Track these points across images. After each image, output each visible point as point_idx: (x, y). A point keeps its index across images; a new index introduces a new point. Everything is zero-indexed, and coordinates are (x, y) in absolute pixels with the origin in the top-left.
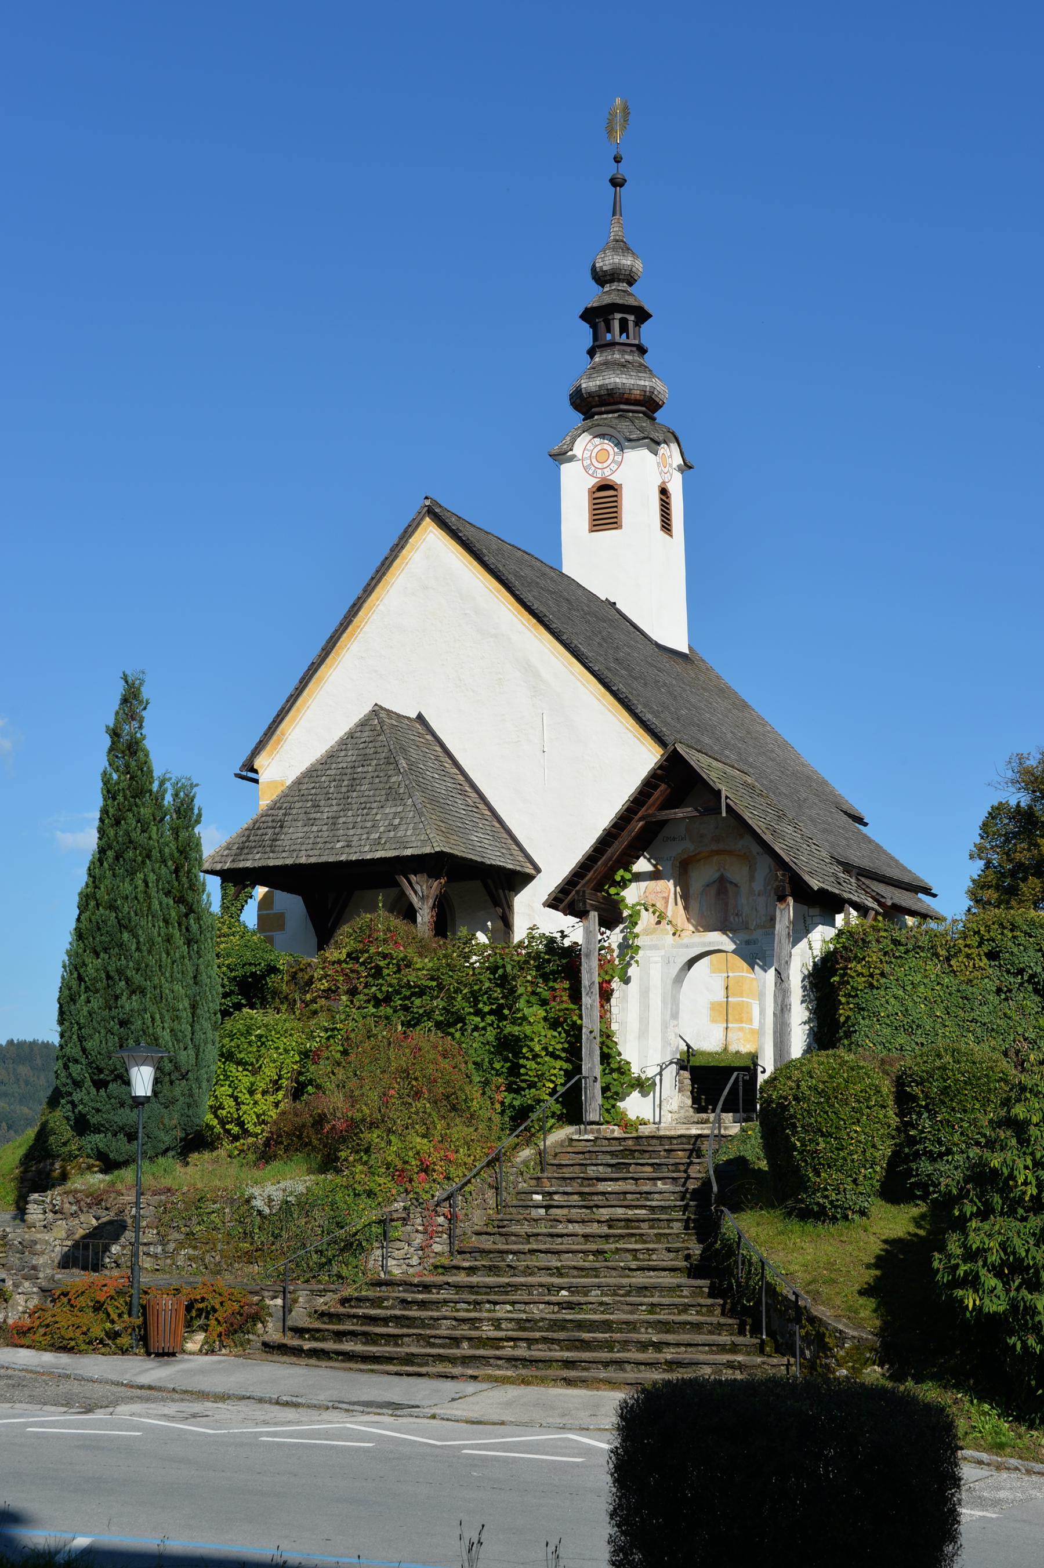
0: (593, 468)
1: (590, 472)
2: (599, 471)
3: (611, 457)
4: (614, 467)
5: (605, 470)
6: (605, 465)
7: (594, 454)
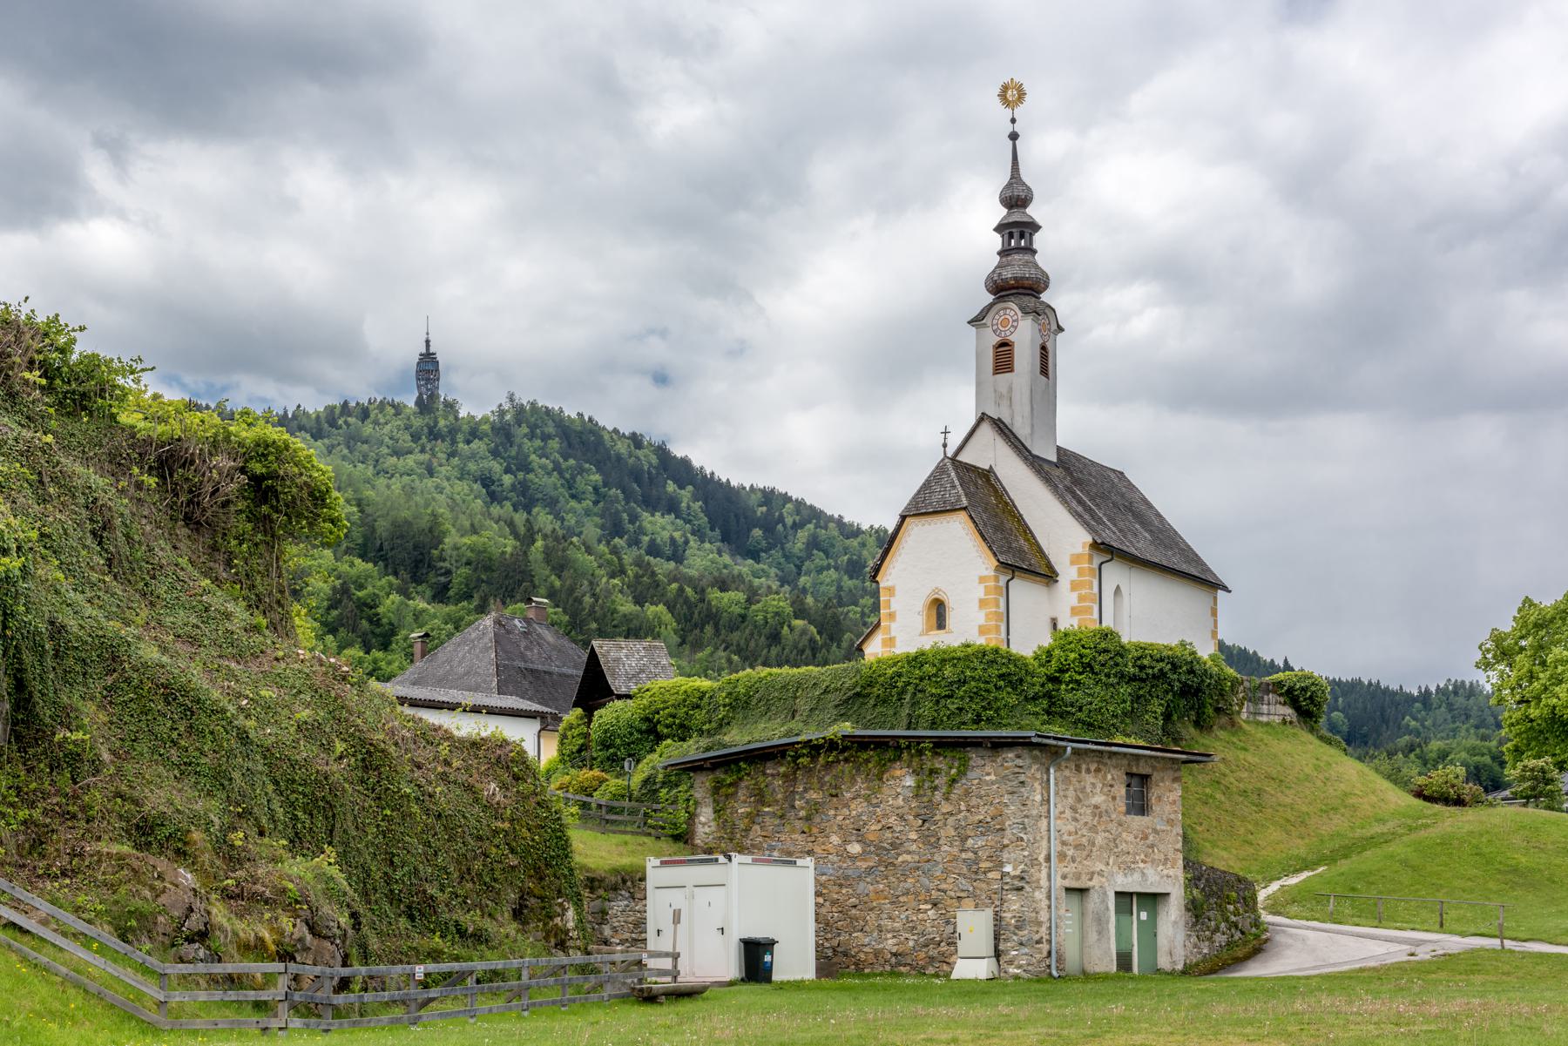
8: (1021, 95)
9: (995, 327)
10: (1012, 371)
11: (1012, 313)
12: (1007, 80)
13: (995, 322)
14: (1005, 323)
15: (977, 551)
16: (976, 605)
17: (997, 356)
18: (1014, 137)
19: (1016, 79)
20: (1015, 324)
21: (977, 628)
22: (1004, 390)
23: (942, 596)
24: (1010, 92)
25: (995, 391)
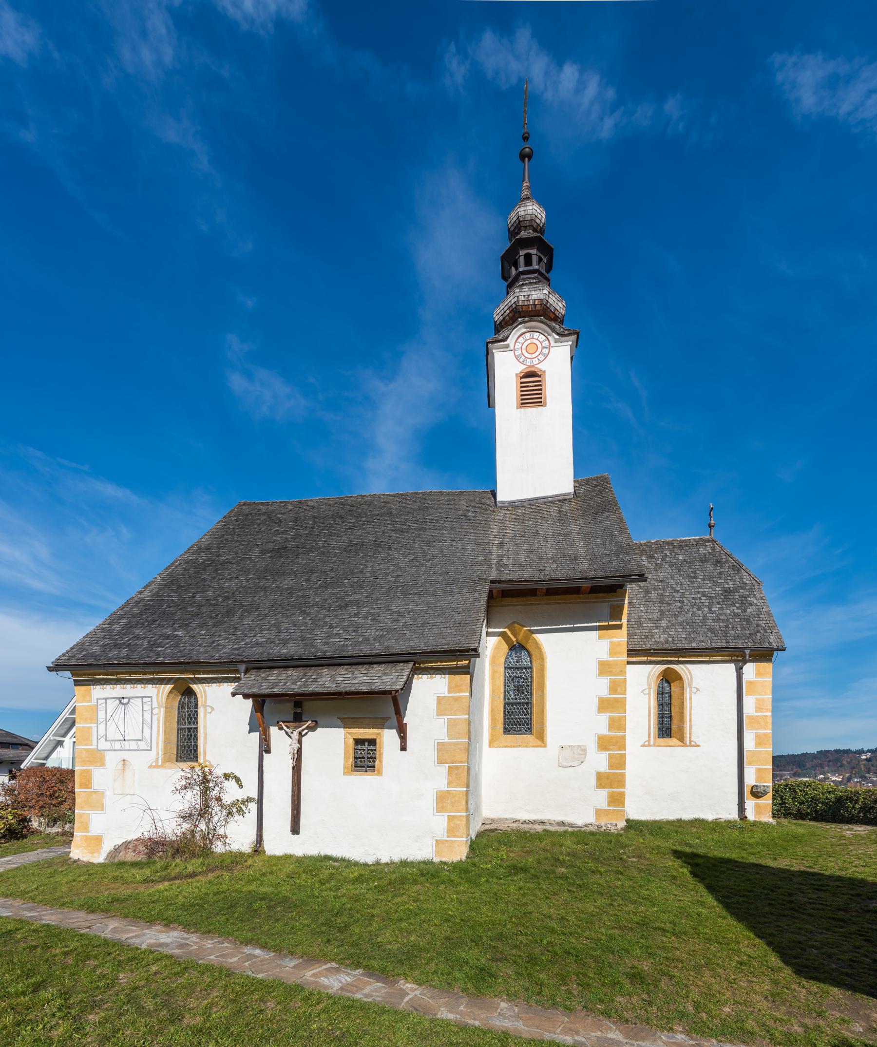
0: (523, 358)
2: (528, 360)
3: (539, 350)
4: (541, 357)
5: (534, 360)
6: (534, 356)
7: (524, 347)
9: (518, 353)
13: (518, 346)
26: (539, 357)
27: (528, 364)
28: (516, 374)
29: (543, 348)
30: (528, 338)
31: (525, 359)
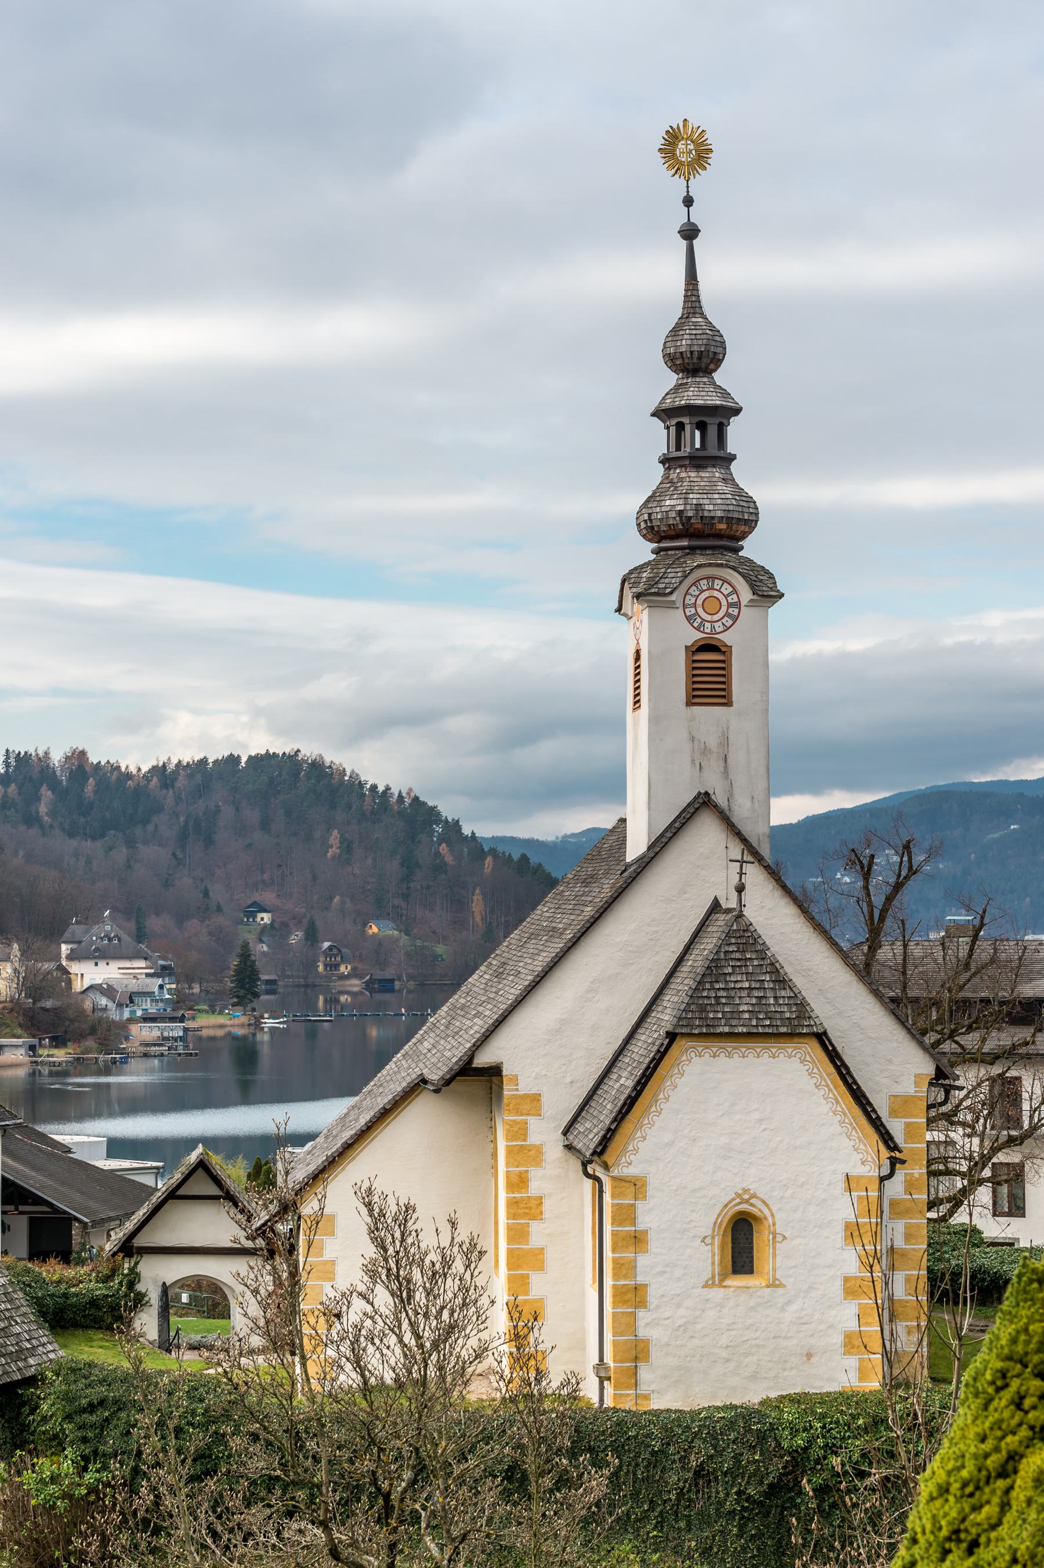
1: (696, 624)
2: (708, 625)
5: (716, 625)
6: (716, 618)
7: (699, 602)
8: (702, 156)
9: (690, 611)
10: (729, 704)
11: (727, 589)
12: (676, 121)
13: (690, 600)
14: (711, 606)
15: (841, 1123)
16: (838, 1234)
17: (694, 669)
18: (690, 233)
19: (693, 122)
20: (734, 611)
21: (839, 1283)
22: (713, 742)
23: (756, 1208)
24: (681, 146)
25: (693, 739)
26: (724, 621)
27: (706, 631)
28: (687, 647)
29: (730, 605)
30: (705, 588)
31: (701, 622)
